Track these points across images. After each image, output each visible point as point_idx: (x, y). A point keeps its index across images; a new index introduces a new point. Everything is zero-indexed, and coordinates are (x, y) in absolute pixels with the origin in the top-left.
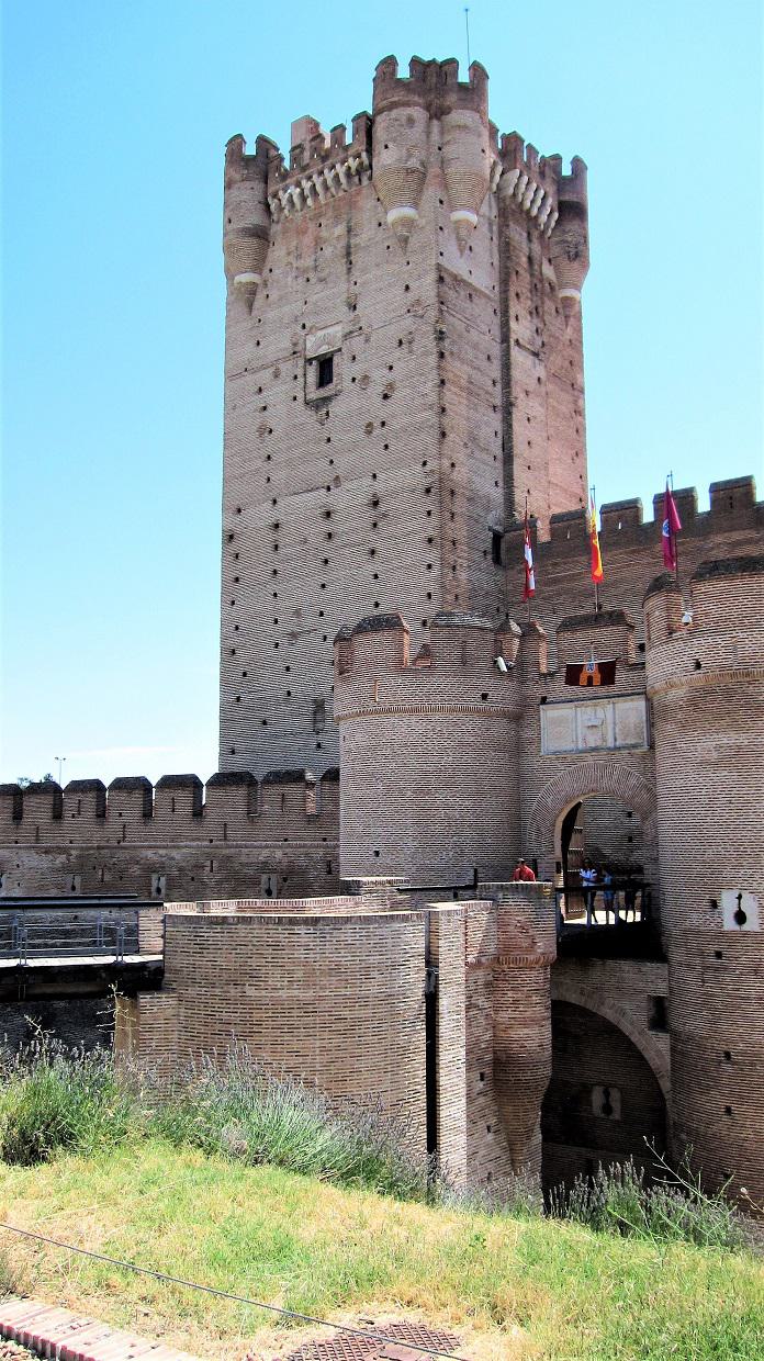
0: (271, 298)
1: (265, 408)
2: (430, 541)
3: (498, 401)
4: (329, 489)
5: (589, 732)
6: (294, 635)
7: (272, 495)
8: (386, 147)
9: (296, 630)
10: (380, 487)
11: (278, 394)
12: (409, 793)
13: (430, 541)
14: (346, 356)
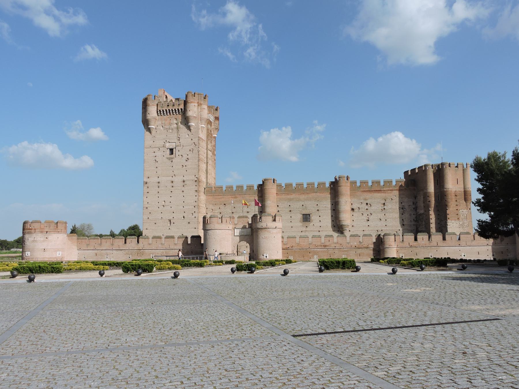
0: (157, 132)
2: (196, 191)
3: (205, 162)
9: (164, 205)
10: (185, 179)
13: (196, 191)
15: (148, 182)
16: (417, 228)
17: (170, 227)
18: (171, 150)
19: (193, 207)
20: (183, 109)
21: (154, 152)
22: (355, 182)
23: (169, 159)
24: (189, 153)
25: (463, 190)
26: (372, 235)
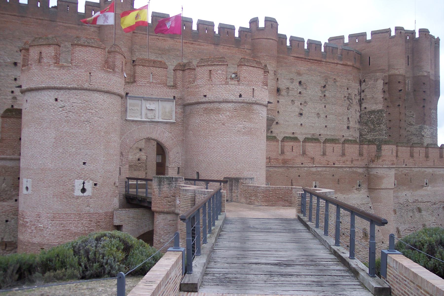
5: (148, 112)
12: (103, 133)
16: (361, 135)
22: (284, 37)
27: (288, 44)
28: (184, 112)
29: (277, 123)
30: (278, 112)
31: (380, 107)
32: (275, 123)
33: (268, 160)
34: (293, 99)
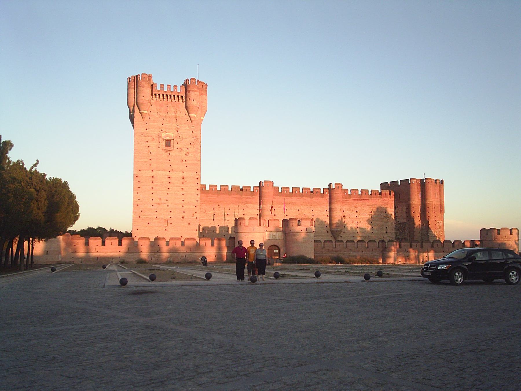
1: (149, 147)
2: (198, 189)
4: (169, 172)
6: (159, 204)
7: (152, 169)
8: (193, 100)
9: (159, 203)
10: (184, 175)
11: (153, 145)
13: (198, 189)
14: (175, 143)
15: (140, 175)
16: (396, 236)
17: (166, 228)
18: (168, 143)
19: (194, 207)
20: (184, 97)
21: (147, 141)
23: (166, 151)
24: (190, 146)
25: (439, 204)
26: (344, 241)
27: (349, 193)
28: (286, 236)
29: (344, 232)
30: (344, 227)
31: (405, 221)
32: (342, 232)
33: (328, 251)
34: (353, 220)
